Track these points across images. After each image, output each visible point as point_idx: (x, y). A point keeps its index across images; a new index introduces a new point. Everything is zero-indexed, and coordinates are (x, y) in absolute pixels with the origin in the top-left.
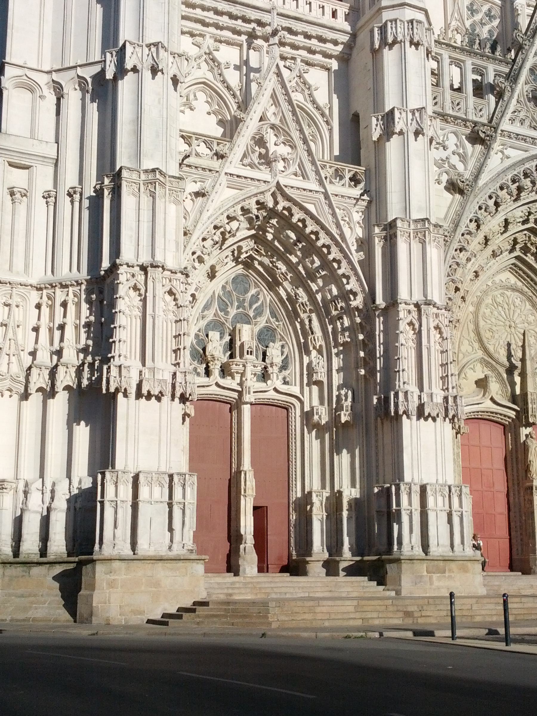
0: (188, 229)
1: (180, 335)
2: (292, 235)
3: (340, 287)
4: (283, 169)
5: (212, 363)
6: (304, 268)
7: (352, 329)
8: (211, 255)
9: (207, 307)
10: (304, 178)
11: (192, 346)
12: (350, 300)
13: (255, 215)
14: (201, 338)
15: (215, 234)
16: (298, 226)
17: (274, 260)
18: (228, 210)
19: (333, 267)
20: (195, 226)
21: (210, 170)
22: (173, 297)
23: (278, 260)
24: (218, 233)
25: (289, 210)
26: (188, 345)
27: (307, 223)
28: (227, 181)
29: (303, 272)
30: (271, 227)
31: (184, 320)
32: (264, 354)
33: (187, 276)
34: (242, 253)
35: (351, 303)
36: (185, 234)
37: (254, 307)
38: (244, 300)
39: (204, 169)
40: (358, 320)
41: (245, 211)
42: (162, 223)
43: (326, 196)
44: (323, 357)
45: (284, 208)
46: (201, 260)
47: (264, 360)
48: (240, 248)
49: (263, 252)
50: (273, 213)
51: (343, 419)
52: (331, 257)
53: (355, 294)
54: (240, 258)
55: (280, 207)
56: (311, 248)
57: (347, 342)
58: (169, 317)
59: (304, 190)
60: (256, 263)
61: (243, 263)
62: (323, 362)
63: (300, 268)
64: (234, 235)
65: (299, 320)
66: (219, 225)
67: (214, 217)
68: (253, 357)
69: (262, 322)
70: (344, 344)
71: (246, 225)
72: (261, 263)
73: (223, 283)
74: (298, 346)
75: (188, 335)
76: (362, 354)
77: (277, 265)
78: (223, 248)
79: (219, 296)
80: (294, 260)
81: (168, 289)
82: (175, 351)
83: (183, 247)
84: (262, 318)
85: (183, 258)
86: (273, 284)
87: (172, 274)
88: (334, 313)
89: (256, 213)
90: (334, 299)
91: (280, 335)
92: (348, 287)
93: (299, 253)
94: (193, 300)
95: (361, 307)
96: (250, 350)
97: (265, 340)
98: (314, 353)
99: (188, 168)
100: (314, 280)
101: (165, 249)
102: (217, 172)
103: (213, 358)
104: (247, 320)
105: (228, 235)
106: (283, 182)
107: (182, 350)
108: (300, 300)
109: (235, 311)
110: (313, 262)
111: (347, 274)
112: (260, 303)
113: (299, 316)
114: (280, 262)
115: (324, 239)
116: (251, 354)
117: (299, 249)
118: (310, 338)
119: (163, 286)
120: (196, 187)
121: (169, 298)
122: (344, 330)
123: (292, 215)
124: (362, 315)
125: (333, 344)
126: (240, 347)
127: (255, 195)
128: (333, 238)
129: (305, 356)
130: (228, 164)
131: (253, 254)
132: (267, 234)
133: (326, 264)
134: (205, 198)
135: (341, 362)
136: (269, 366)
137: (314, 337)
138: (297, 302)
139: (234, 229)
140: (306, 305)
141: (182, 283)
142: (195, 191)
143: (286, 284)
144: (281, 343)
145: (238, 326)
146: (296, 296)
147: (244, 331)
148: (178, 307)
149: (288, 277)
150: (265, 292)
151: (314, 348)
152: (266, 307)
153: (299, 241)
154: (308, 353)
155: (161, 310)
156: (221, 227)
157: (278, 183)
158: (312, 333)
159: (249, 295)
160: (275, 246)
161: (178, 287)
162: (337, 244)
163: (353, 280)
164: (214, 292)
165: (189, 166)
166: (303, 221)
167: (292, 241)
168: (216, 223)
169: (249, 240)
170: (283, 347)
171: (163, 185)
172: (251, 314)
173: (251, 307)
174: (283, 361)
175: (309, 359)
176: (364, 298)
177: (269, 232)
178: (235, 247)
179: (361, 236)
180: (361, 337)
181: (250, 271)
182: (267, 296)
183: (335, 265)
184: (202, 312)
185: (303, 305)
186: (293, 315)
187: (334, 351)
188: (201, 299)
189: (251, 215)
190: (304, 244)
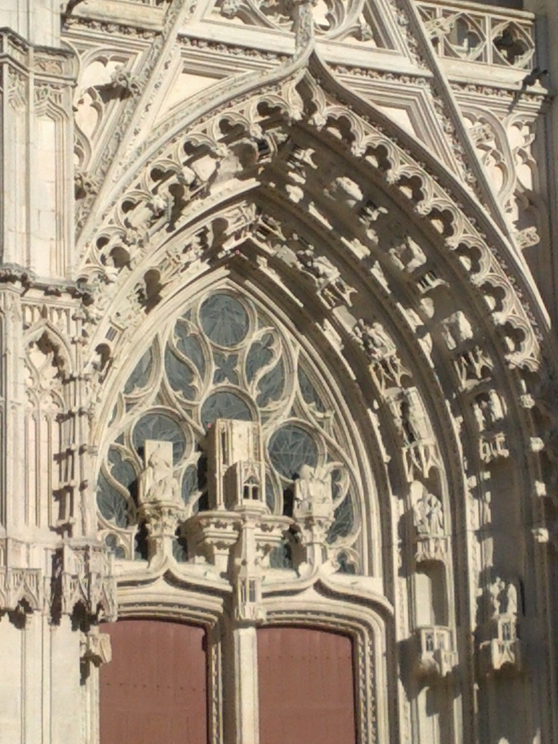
0: (86, 179)
1: (70, 452)
2: (354, 190)
3: (480, 317)
4: (326, 23)
5: (154, 521)
6: (387, 271)
7: (514, 427)
8: (147, 247)
9: (138, 378)
10: (379, 43)
11: (103, 480)
12: (506, 351)
13: (256, 140)
14: (124, 457)
15: (155, 191)
16: (369, 165)
17: (308, 252)
18: (186, 128)
19: (460, 265)
20: (104, 174)
21: (140, 31)
22: (52, 355)
23: (317, 253)
24: (164, 189)
25: (343, 124)
26: (92, 476)
27: (391, 155)
28: (183, 55)
29: (384, 283)
30: (297, 170)
31: (81, 413)
32: (289, 496)
33: (87, 300)
34: (226, 238)
35: (508, 357)
36: (80, 193)
37: (260, 374)
38: (234, 358)
39: (123, 28)
40: (528, 401)
41: (231, 130)
42: (20, 167)
43: (437, 86)
44: (439, 498)
45: (331, 121)
46: (120, 259)
47: (288, 510)
48: (220, 225)
49: (278, 233)
50: (301, 133)
51: (499, 659)
52: (453, 242)
53: (518, 336)
54: (221, 249)
55: (319, 119)
56: (401, 220)
57: (501, 457)
58: (44, 407)
59: (381, 73)
60: (262, 263)
61: (228, 262)
62: (441, 513)
63: (376, 272)
64: (204, 194)
65: (376, 405)
66: (167, 167)
67: (151, 149)
68: (261, 504)
69: (281, 413)
70: (496, 465)
71: (232, 165)
72: (275, 263)
73: (178, 315)
74: (374, 471)
75: (93, 453)
76: (541, 489)
77: (316, 264)
78: (178, 226)
79: (169, 348)
80: (360, 251)
81: (37, 334)
82: (59, 495)
83: (74, 227)
84: (281, 403)
85: (74, 254)
86: (307, 316)
87: (49, 297)
88: (466, 384)
89: (259, 136)
90: (465, 349)
91: (329, 443)
92: (500, 318)
93: (371, 234)
94: (103, 361)
95: (534, 367)
96: (251, 486)
97: (288, 458)
98: (417, 490)
99: (83, 27)
100: (412, 302)
101: (28, 234)
102: (158, 33)
103: (158, 508)
104: (242, 408)
105: (188, 194)
106: (326, 53)
107: (77, 493)
108: (378, 353)
109: (211, 387)
110: (408, 256)
111: (496, 284)
112: (274, 363)
113: (376, 394)
114: (323, 259)
115: (433, 198)
116: (255, 497)
117: (373, 225)
118: (405, 450)
119: (26, 327)
120: (103, 74)
121: (39, 358)
122: (492, 427)
123: (350, 137)
124: (538, 388)
125: (464, 465)
126: (225, 477)
127: (257, 90)
128: (456, 192)
129: (393, 499)
130: (184, 13)
131: (255, 240)
132: (289, 188)
133: (441, 260)
134: (129, 102)
135: (488, 511)
136: (302, 526)
137: (416, 449)
138: (370, 360)
139: (205, 176)
140: (394, 366)
141: (74, 318)
142: (102, 83)
143: (340, 313)
144: (330, 466)
145: (221, 424)
146: (366, 344)
147: (235, 437)
148: (65, 382)
149: (346, 296)
150: (288, 335)
151: (418, 476)
152: (291, 372)
153: (370, 202)
154: (402, 490)
155: (21, 389)
156: (170, 173)
157: (313, 57)
158: (412, 438)
159: (247, 344)
160: (311, 217)
161: (65, 329)
162: (469, 209)
163: (512, 299)
164: (156, 340)
165: (86, 21)
166: (380, 152)
167: (352, 203)
168: (159, 161)
169: (243, 203)
170: (336, 475)
171: (20, 71)
172: (253, 393)
173: (251, 375)
174: (337, 512)
175: (406, 506)
176: (542, 344)
177: (293, 183)
178: (207, 222)
179: (528, 185)
180: (537, 445)
181: (248, 283)
182: (292, 347)
183: (466, 262)
184: (128, 390)
185: (385, 366)
186: (360, 394)
187: (469, 482)
188: (123, 358)
189: (246, 141)
190: (384, 210)
